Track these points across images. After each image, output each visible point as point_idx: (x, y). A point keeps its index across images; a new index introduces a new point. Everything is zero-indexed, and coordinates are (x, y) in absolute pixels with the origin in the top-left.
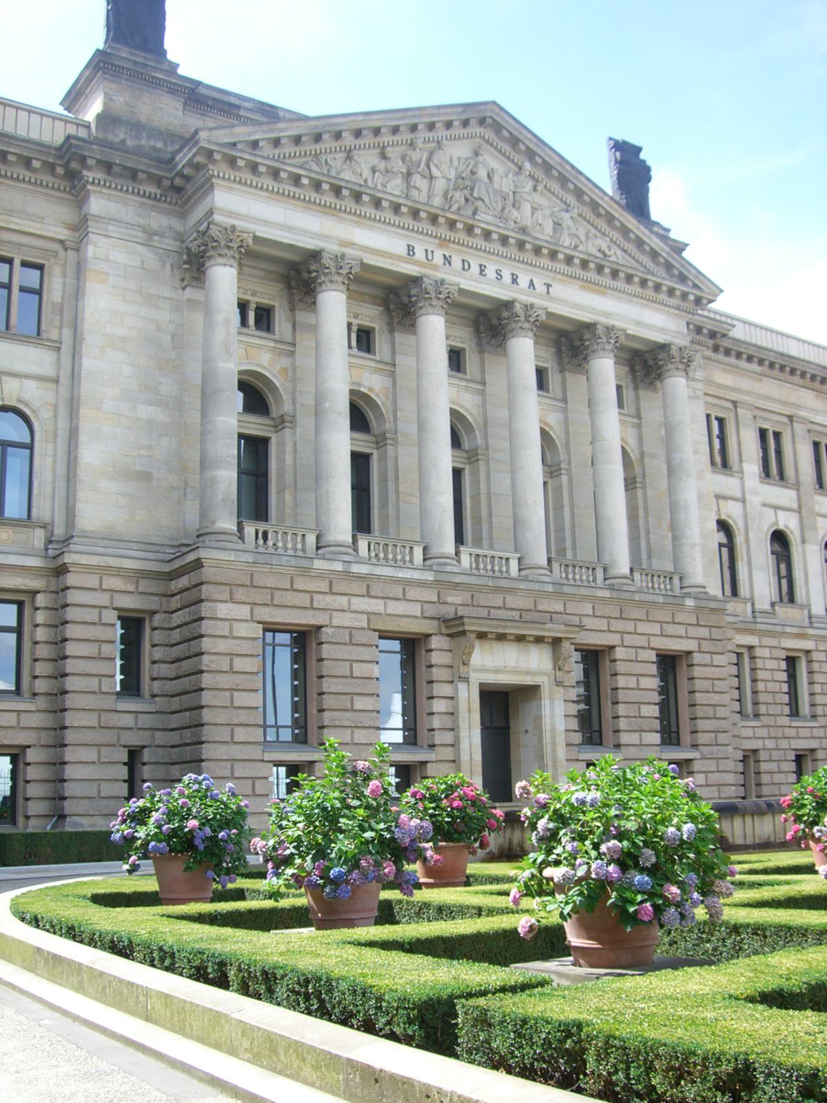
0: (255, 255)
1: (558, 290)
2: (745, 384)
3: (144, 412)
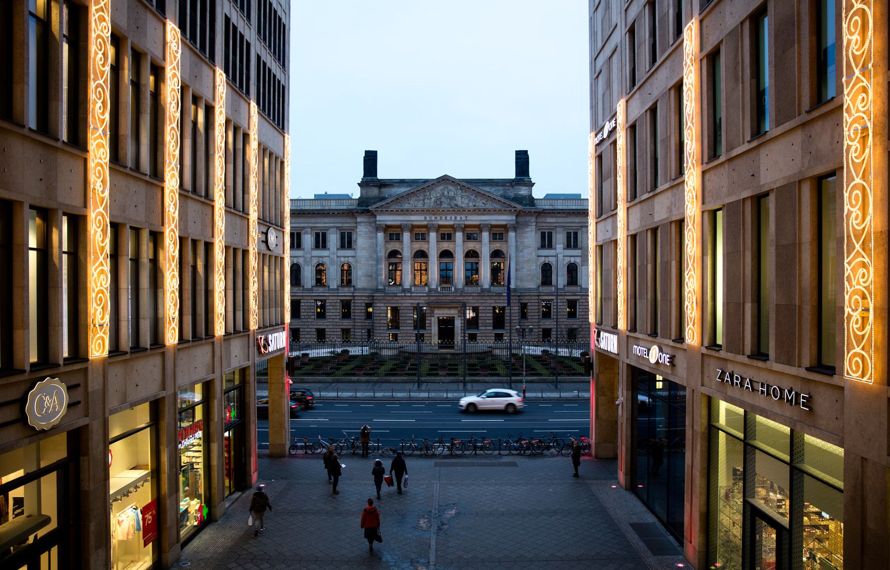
0: (387, 228)
1: (470, 217)
2: (560, 220)
3: (370, 262)
